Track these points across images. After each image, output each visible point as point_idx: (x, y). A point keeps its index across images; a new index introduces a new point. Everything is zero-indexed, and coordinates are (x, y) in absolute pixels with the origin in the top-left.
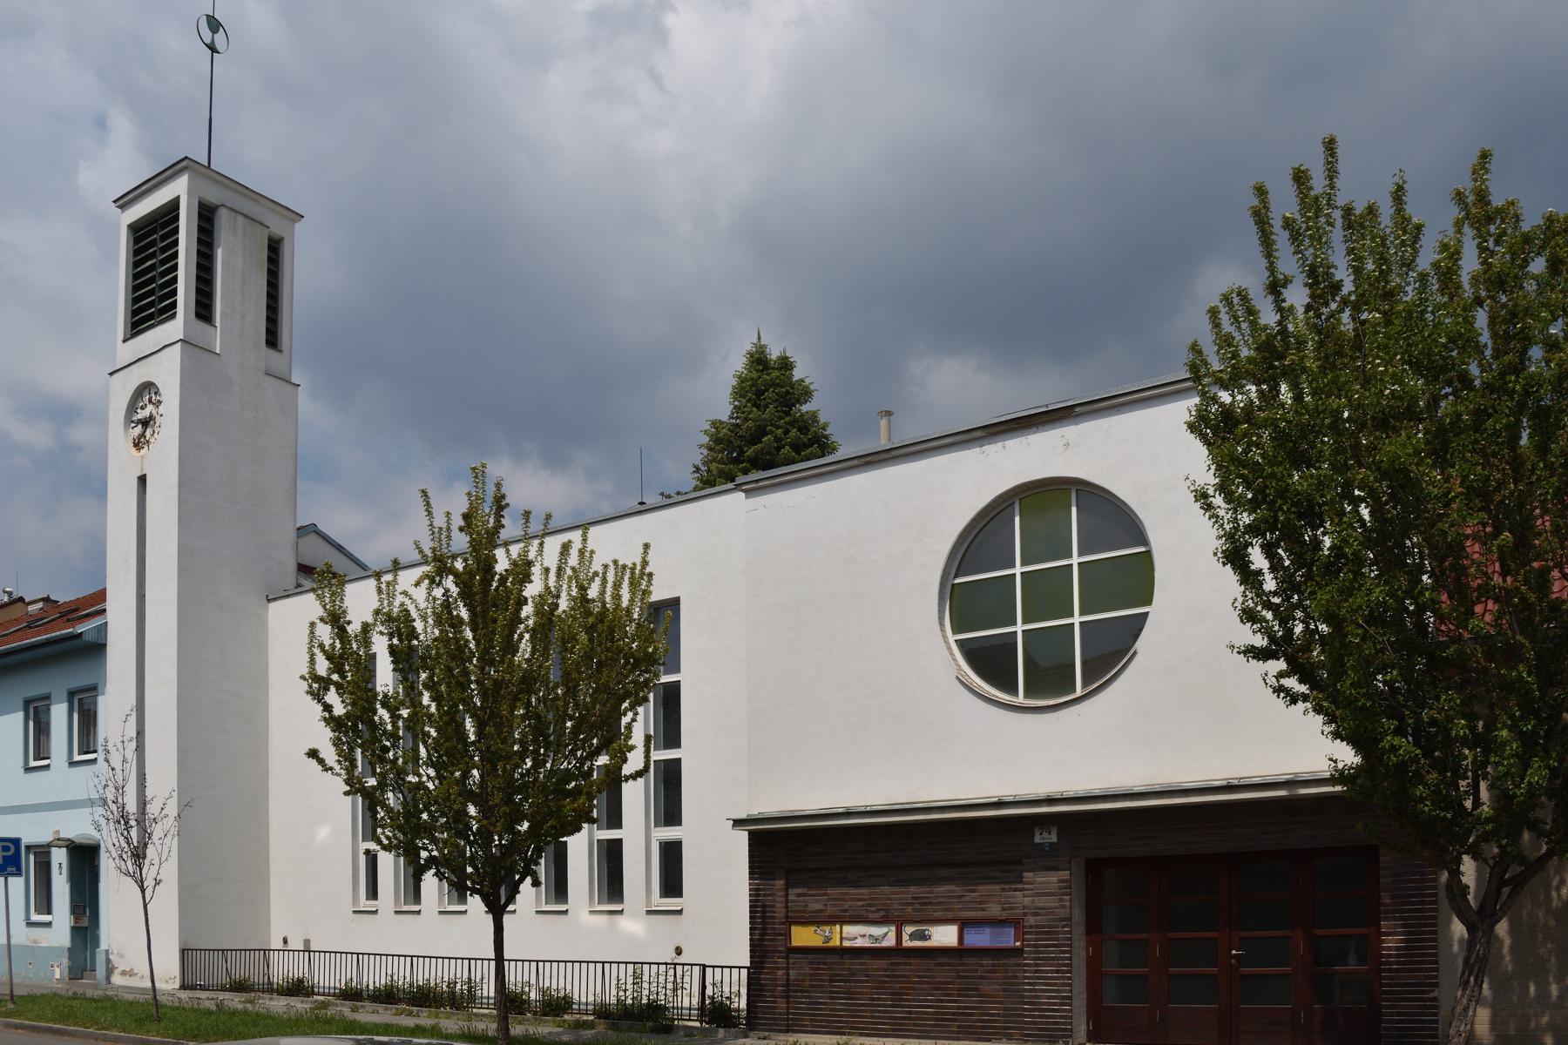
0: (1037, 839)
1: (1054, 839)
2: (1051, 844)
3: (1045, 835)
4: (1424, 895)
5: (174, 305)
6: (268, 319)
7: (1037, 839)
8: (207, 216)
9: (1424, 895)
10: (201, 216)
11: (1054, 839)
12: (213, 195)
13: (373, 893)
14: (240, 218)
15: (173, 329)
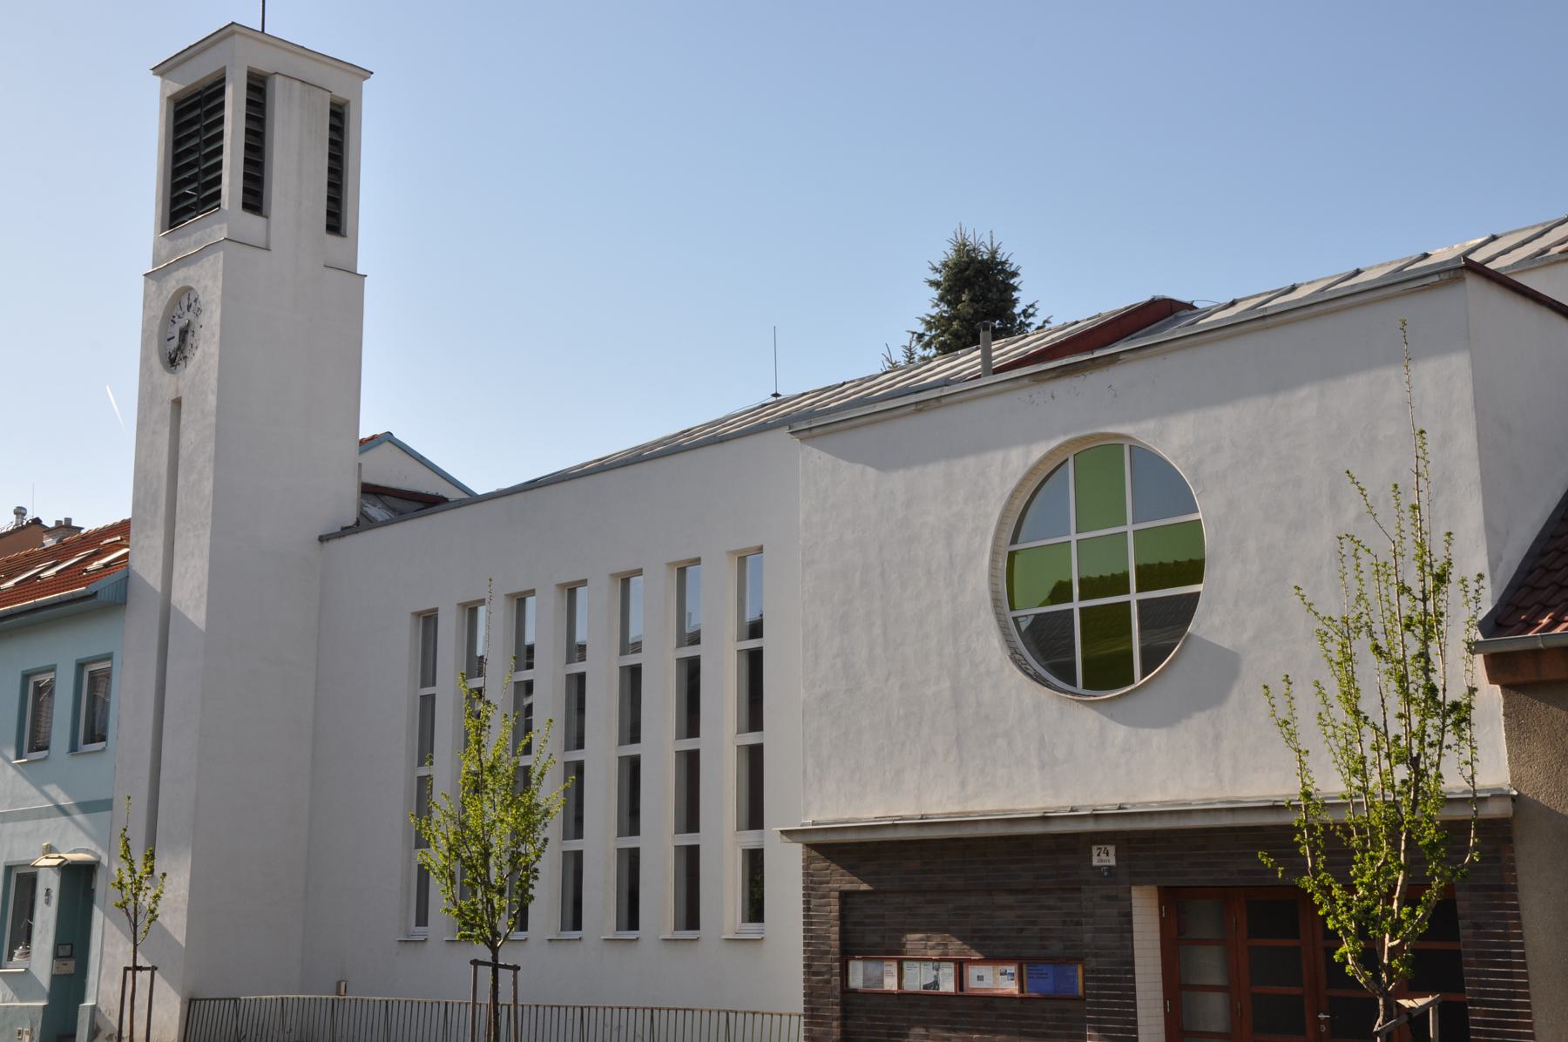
0: (1095, 862)
1: (1113, 862)
2: (1110, 867)
3: (1103, 856)
4: (1509, 955)
5: (218, 195)
6: (329, 213)
7: (1095, 862)
8: (258, 88)
9: (1509, 955)
10: (250, 87)
11: (1113, 862)
12: (263, 66)
13: (422, 920)
14: (297, 84)
15: (209, 229)
